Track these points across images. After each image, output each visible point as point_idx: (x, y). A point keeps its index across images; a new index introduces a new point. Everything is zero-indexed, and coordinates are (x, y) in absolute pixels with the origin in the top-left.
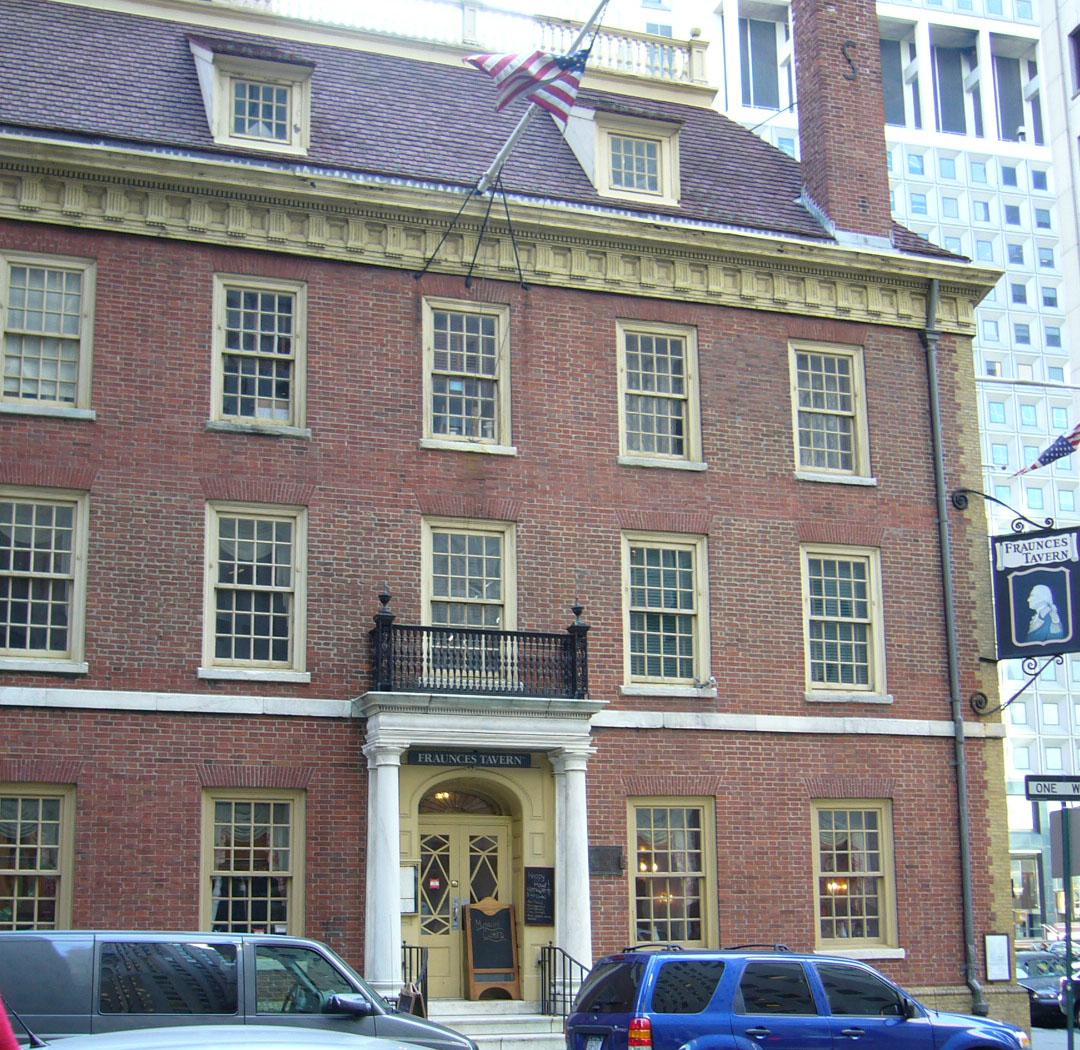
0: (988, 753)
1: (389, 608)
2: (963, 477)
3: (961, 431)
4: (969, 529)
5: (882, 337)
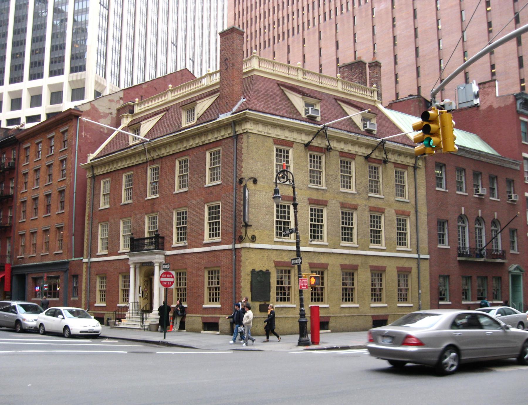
0: (243, 252)
1: (134, 236)
5: (225, 141)
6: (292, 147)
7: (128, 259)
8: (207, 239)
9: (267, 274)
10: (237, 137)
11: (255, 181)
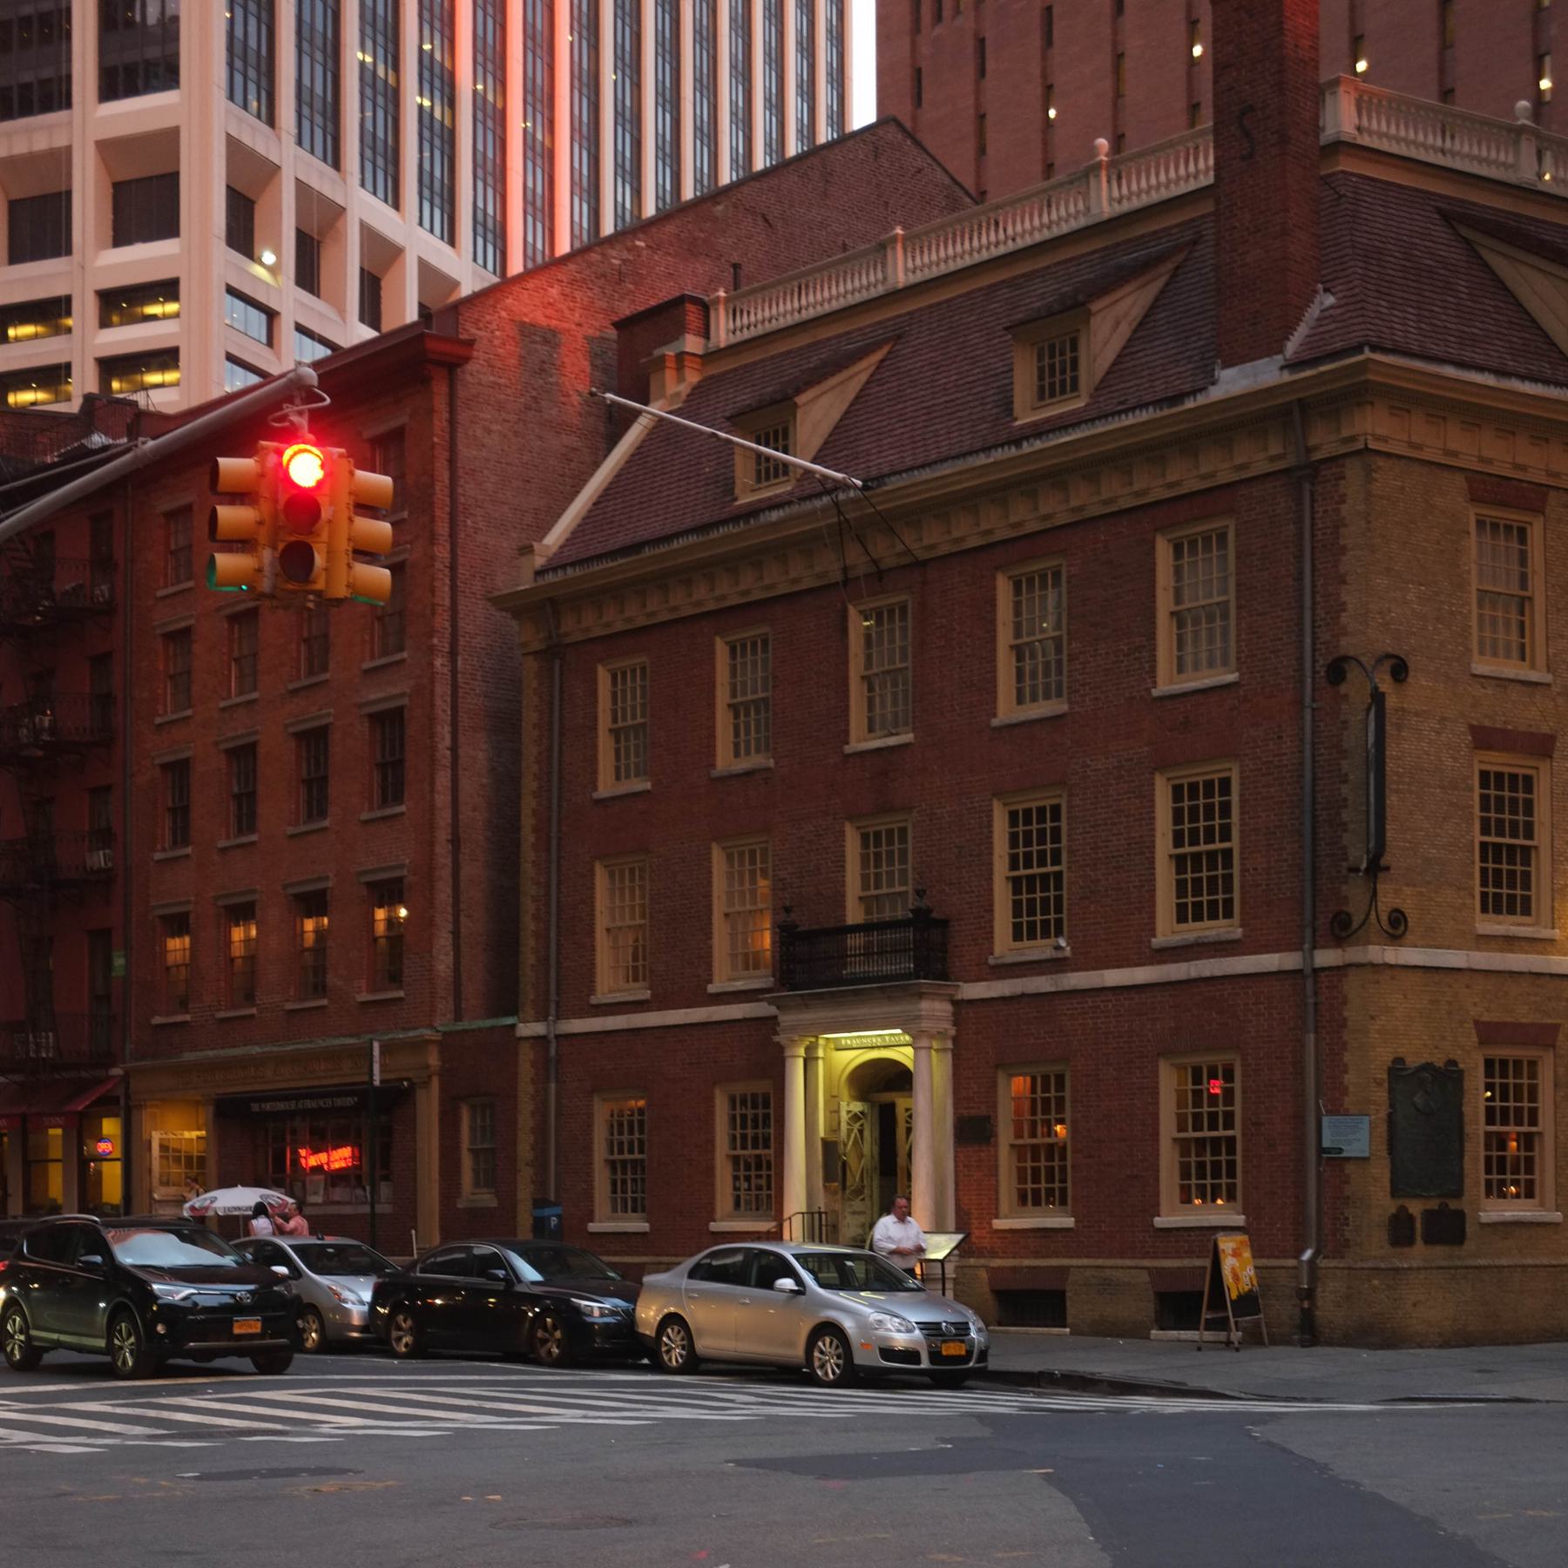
2: (1343, 642)
3: (1344, 582)
4: (1344, 706)
6: (1538, 509)
7: (775, 1017)
8: (1167, 930)
9: (1448, 1078)
10: (1308, 475)
11: (1400, 671)
